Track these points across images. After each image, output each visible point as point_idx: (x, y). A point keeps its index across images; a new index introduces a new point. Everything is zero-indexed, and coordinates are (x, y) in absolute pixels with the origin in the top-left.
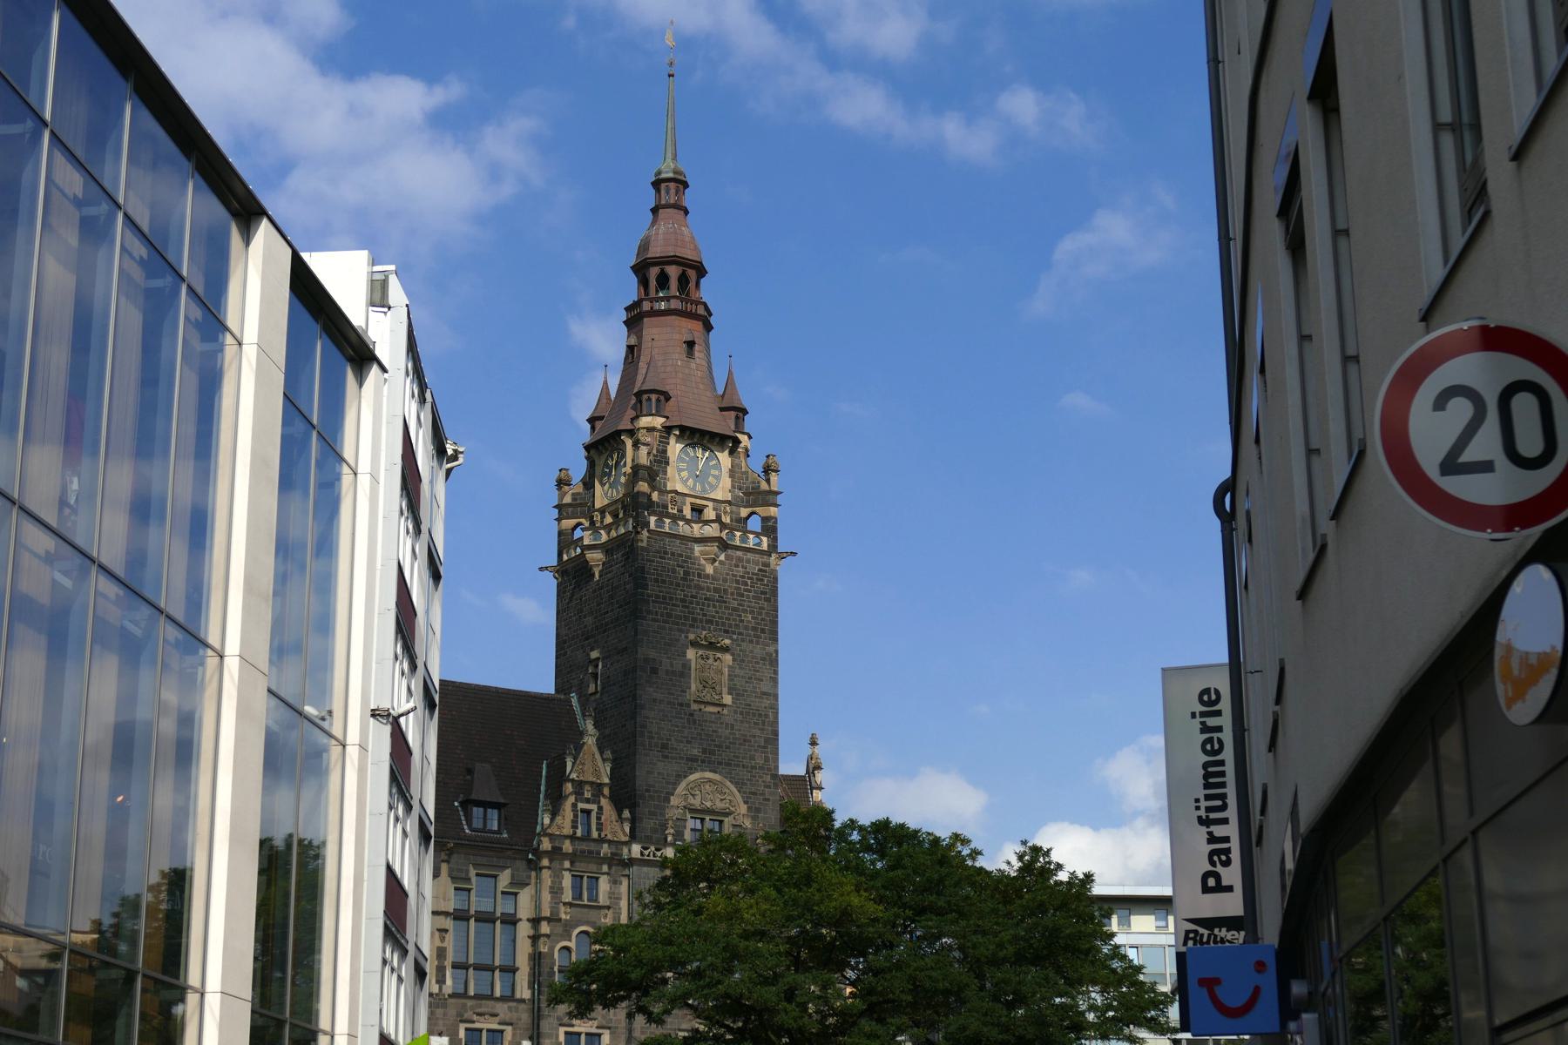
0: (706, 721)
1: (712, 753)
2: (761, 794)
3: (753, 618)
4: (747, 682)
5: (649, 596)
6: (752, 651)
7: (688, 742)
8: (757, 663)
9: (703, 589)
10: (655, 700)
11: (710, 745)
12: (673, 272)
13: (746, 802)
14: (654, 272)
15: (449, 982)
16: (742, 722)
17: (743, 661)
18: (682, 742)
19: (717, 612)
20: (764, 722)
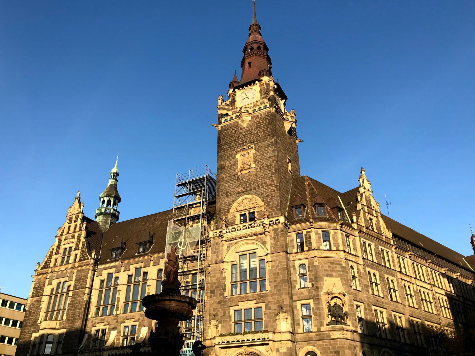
0: (245, 177)
1: (247, 187)
2: (270, 195)
3: (264, 133)
4: (262, 156)
5: (221, 145)
6: (264, 145)
7: (237, 187)
8: (267, 147)
9: (242, 133)
10: (223, 178)
11: (247, 185)
13: (262, 201)
16: (260, 171)
17: (260, 149)
18: (234, 188)
19: (248, 138)
20: (270, 168)
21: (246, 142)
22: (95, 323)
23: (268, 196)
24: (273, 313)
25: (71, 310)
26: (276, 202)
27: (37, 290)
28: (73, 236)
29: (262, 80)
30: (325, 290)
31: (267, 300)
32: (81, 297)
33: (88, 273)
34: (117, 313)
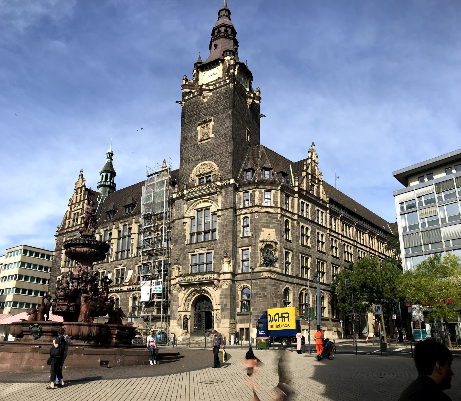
6: (222, 117)
8: (224, 119)
13: (218, 166)
15: (134, 253)
17: (218, 121)
21: (206, 115)
22: (97, 268)
23: (222, 162)
24: (220, 257)
26: (229, 166)
29: (225, 59)
30: (261, 239)
31: (216, 247)
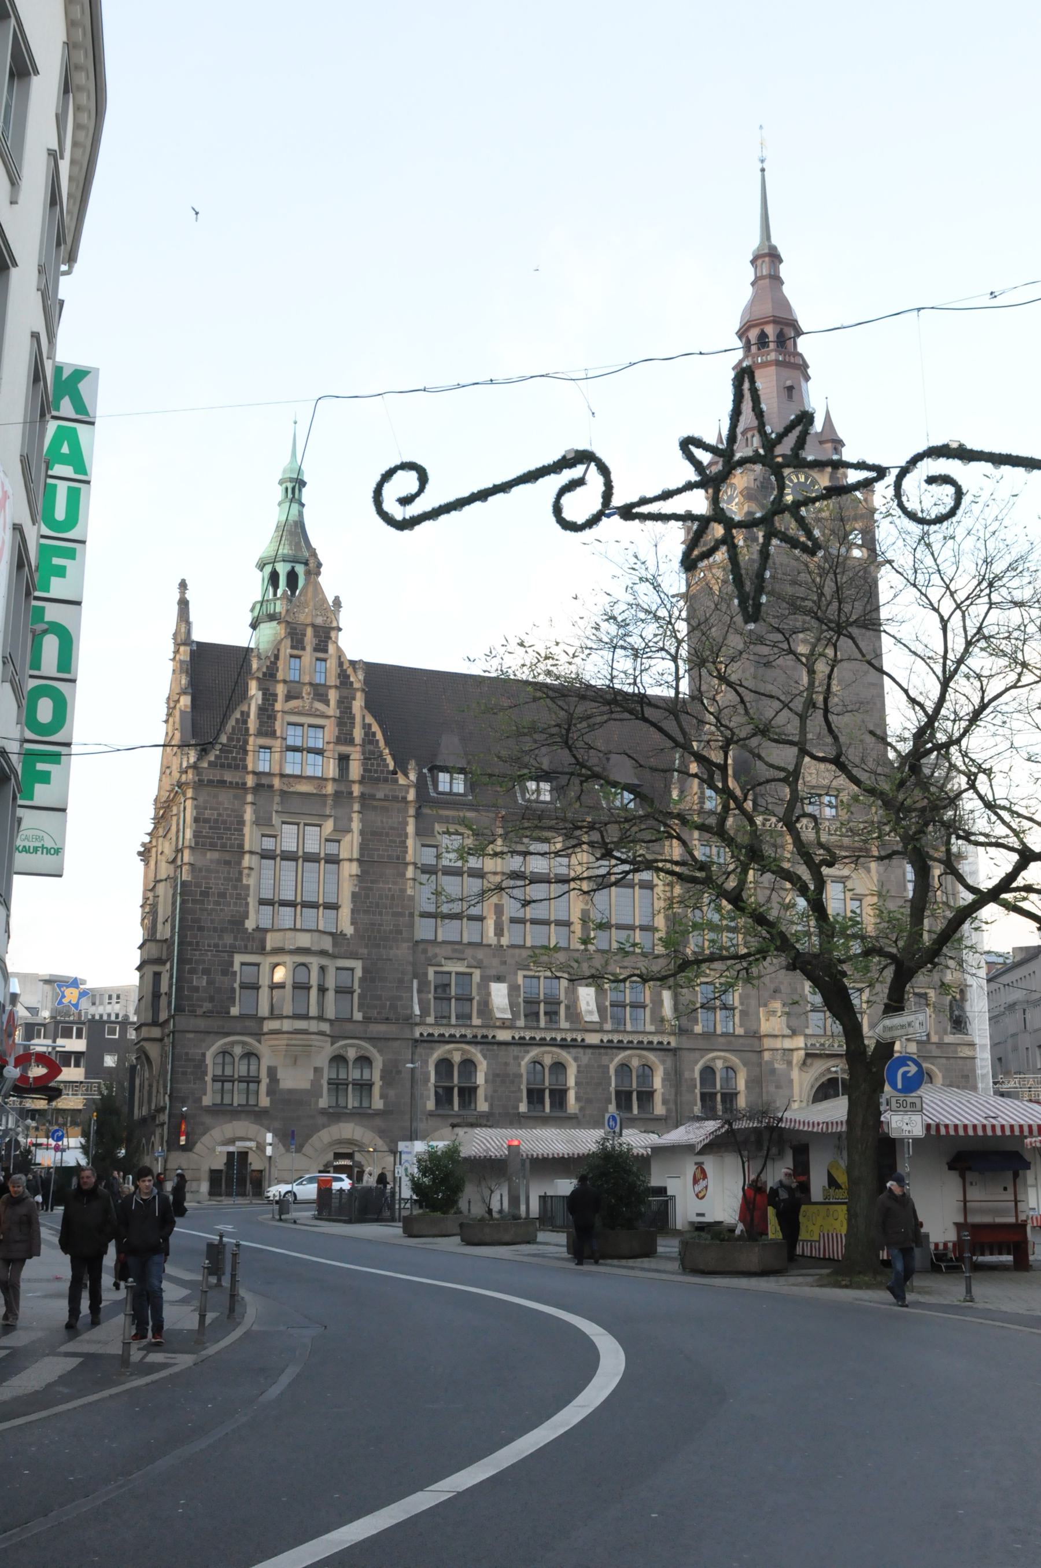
12: (770, 330)
14: (753, 334)
25: (366, 912)
27: (211, 828)
28: (322, 695)
32: (394, 883)
33: (407, 824)
34: (499, 940)
